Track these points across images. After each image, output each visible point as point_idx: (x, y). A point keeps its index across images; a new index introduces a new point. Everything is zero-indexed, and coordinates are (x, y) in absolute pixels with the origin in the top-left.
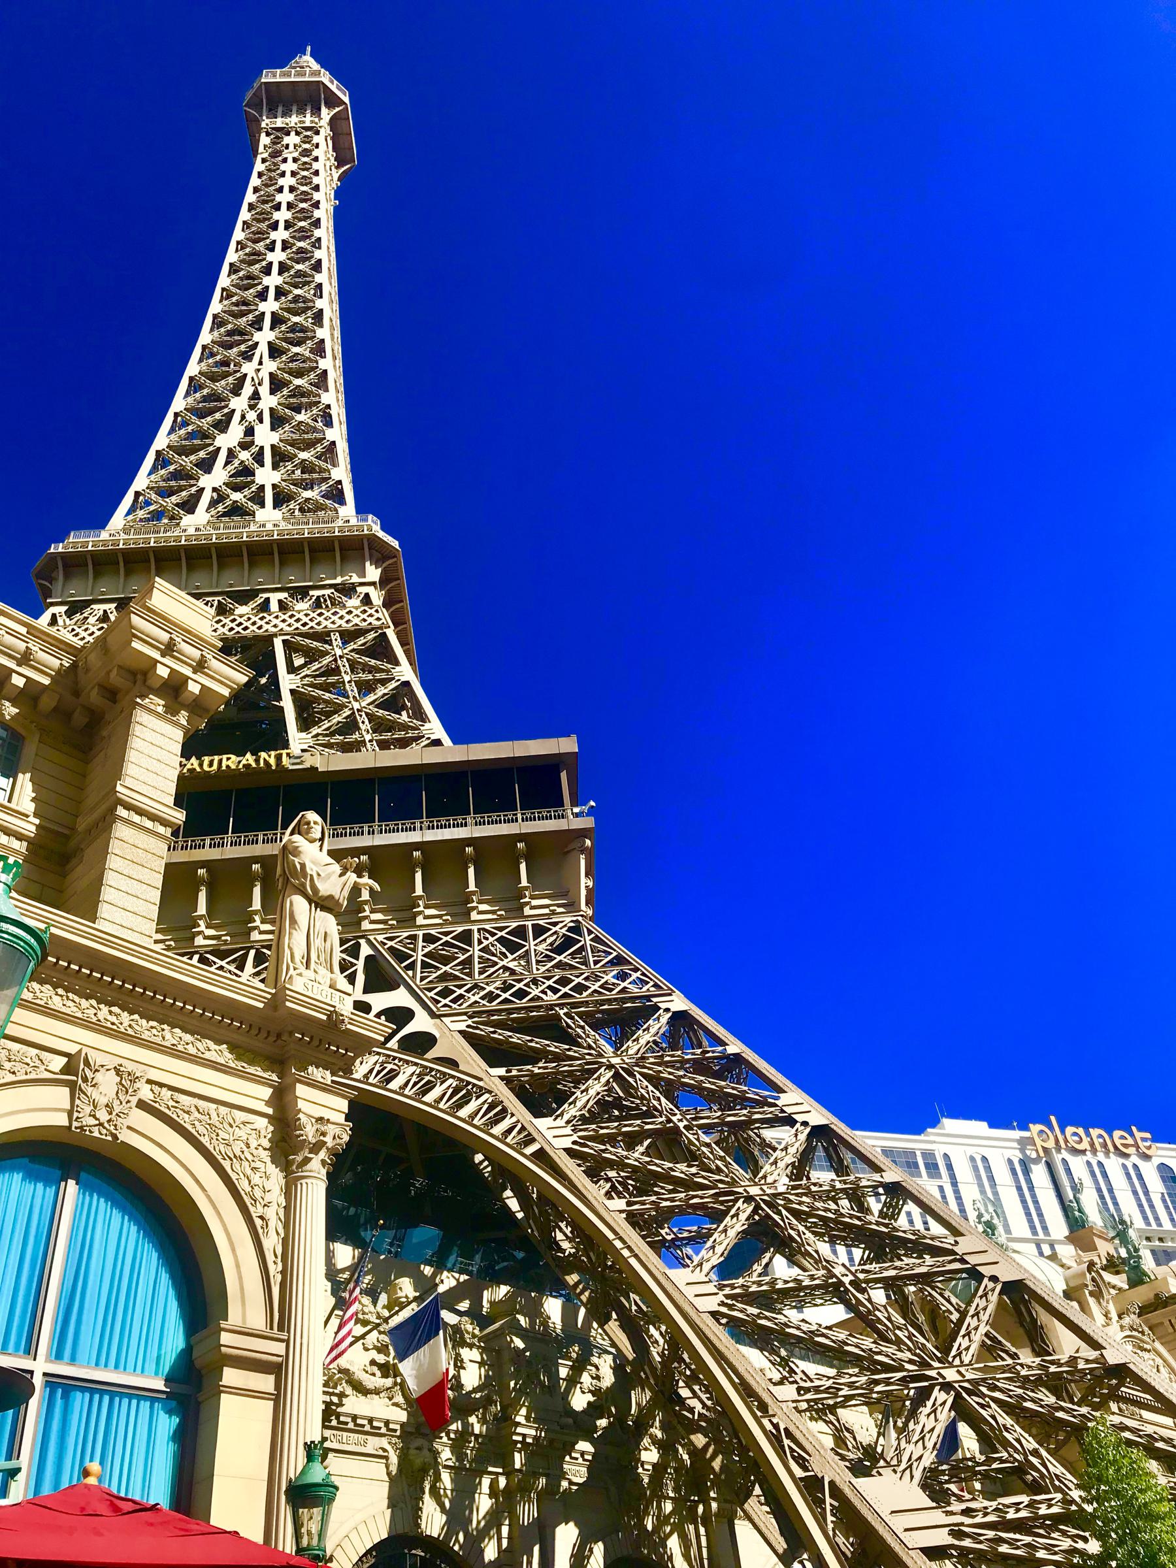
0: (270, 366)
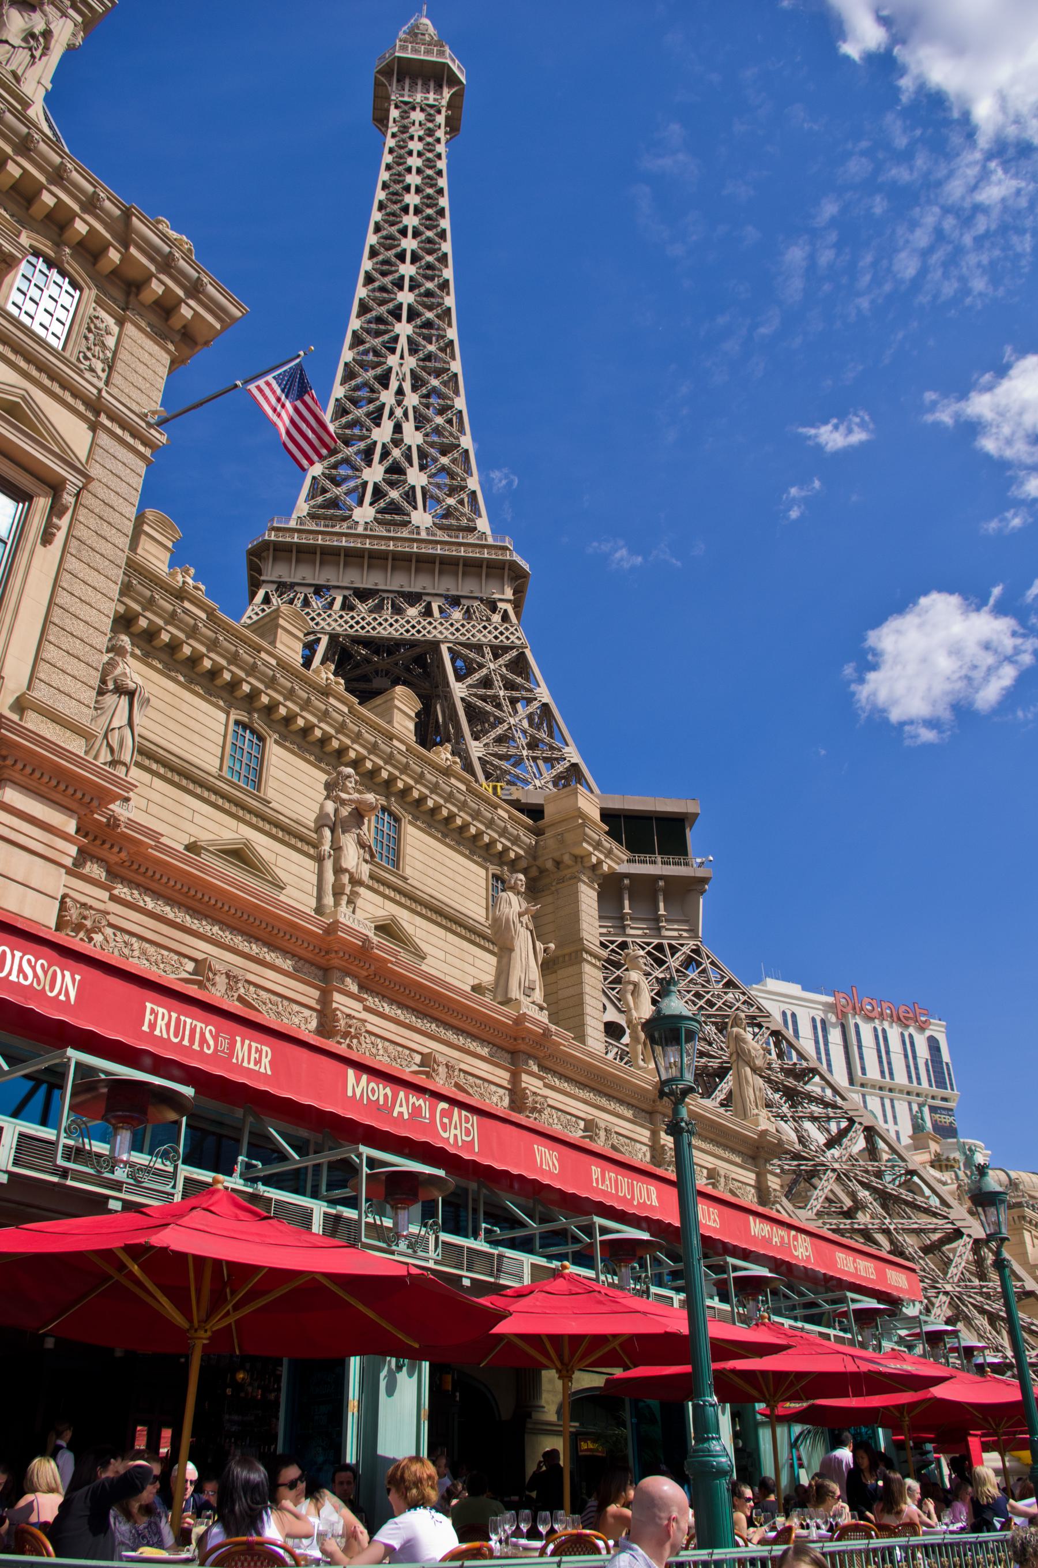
0: (411, 362)
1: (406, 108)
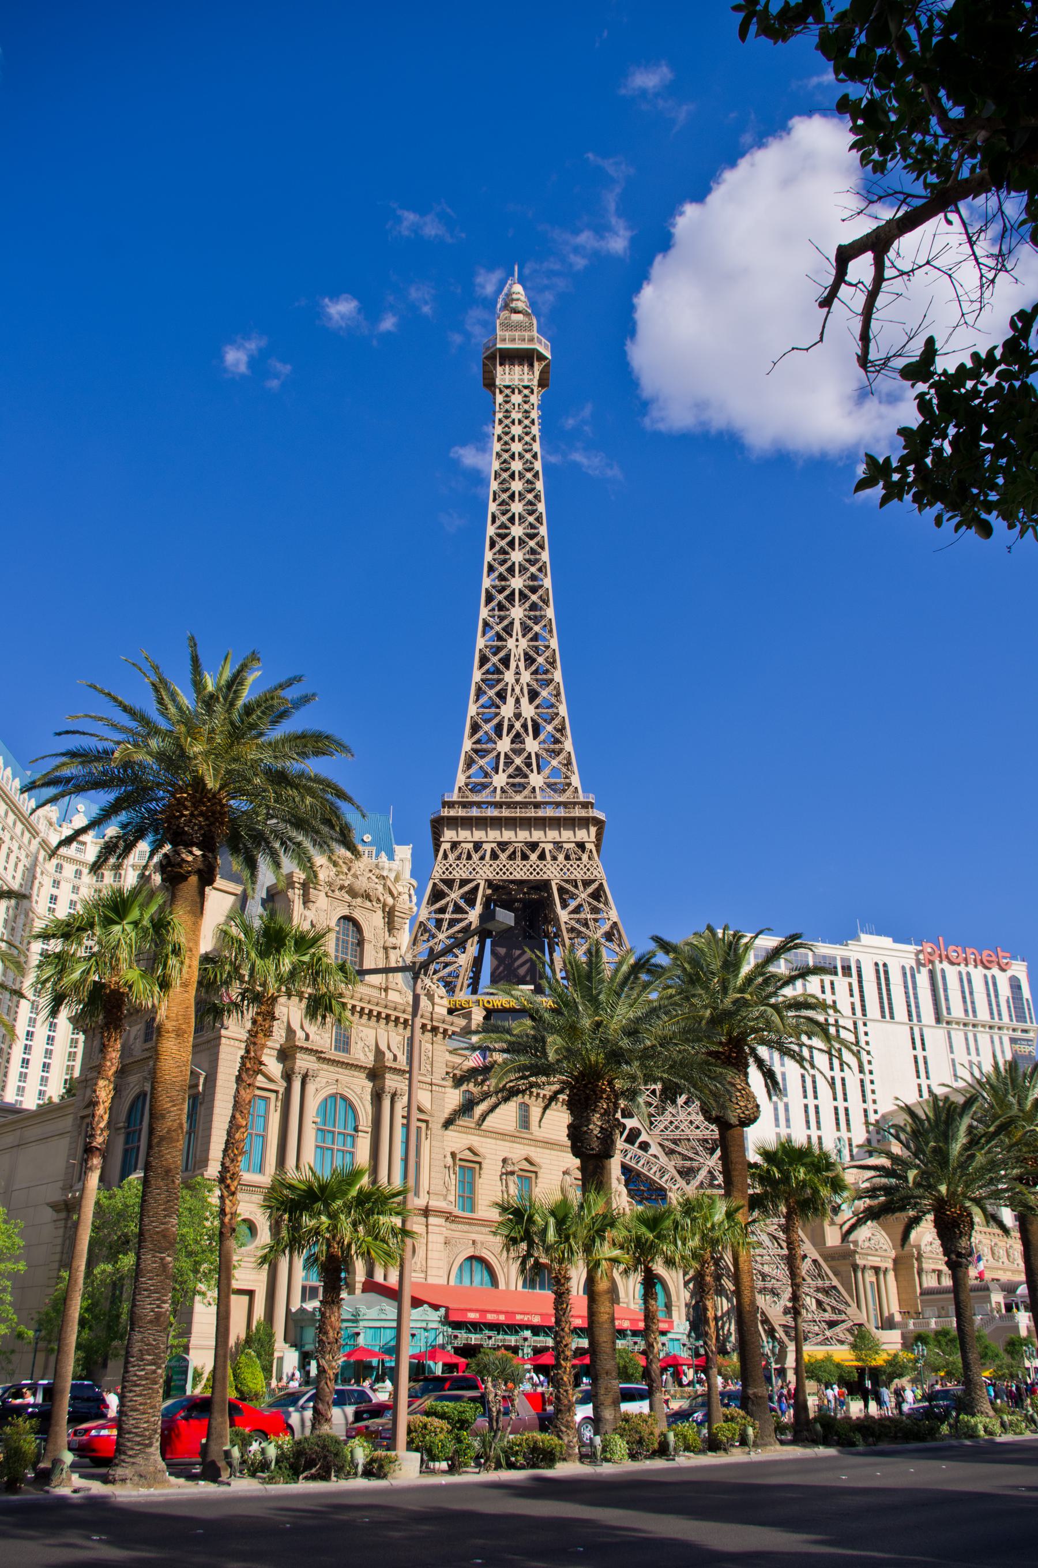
1: (508, 391)
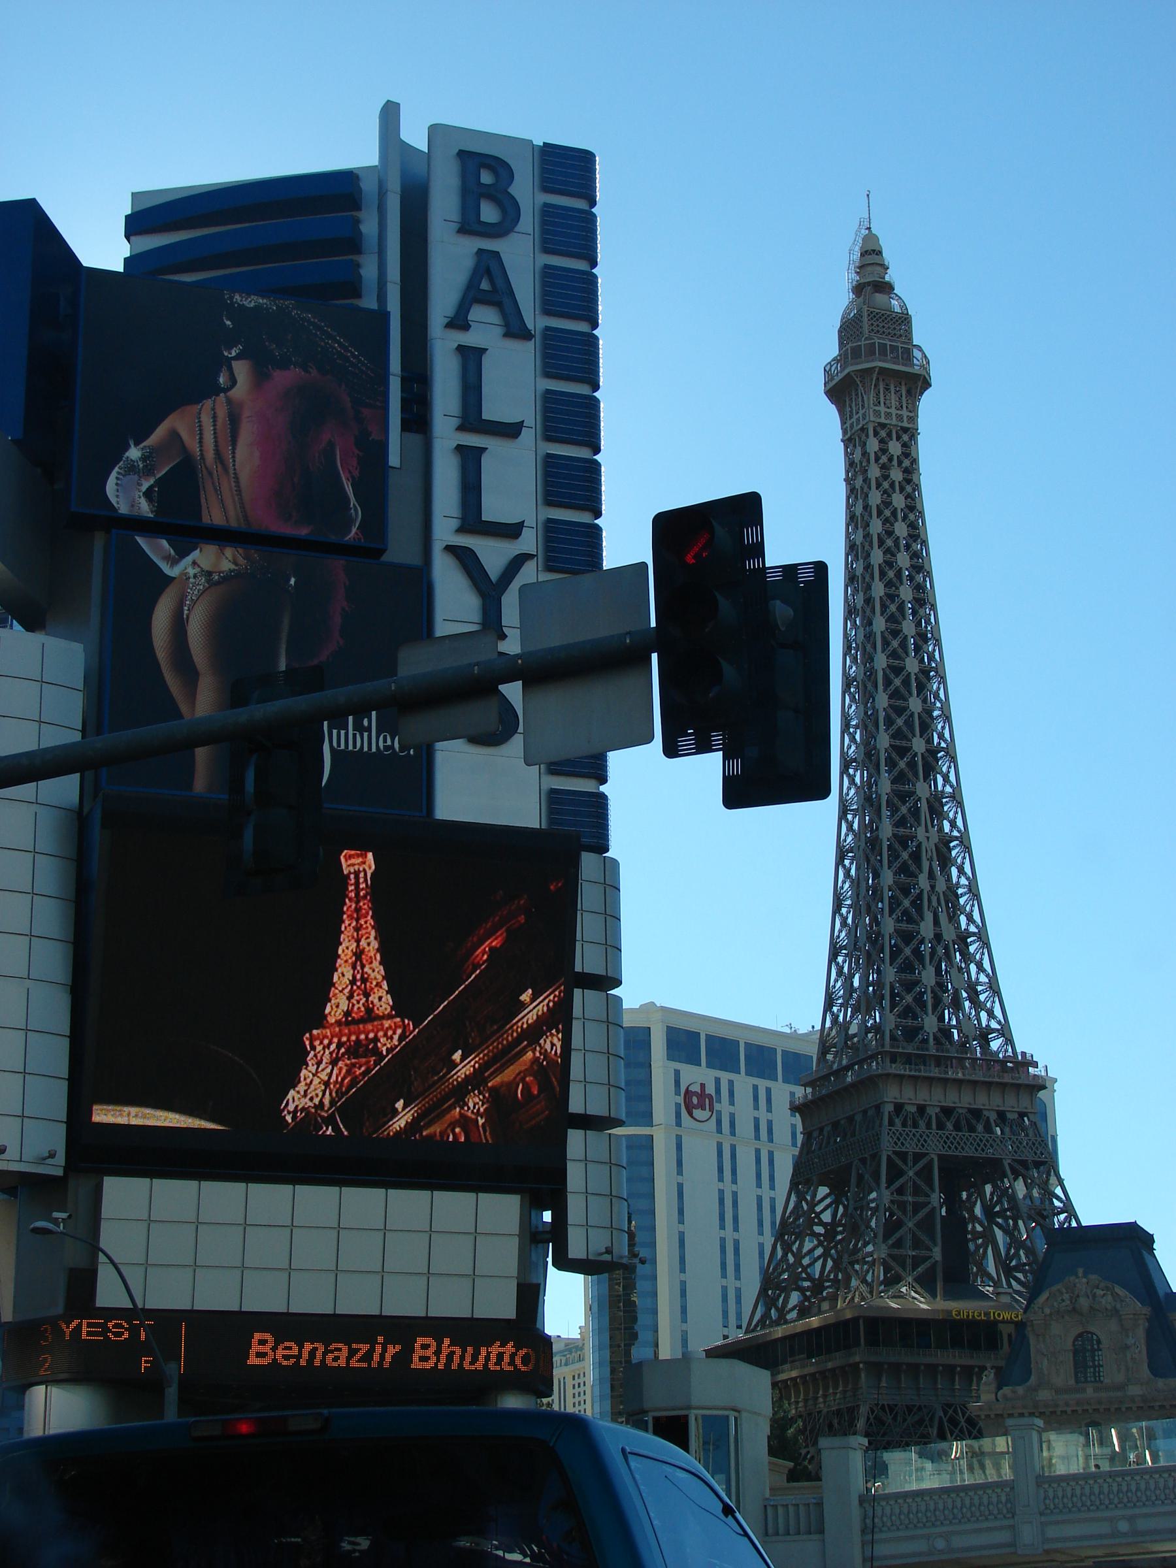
1: (883, 434)
